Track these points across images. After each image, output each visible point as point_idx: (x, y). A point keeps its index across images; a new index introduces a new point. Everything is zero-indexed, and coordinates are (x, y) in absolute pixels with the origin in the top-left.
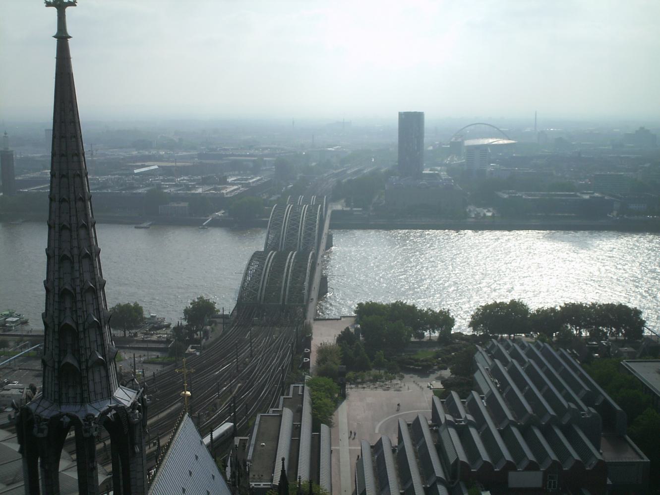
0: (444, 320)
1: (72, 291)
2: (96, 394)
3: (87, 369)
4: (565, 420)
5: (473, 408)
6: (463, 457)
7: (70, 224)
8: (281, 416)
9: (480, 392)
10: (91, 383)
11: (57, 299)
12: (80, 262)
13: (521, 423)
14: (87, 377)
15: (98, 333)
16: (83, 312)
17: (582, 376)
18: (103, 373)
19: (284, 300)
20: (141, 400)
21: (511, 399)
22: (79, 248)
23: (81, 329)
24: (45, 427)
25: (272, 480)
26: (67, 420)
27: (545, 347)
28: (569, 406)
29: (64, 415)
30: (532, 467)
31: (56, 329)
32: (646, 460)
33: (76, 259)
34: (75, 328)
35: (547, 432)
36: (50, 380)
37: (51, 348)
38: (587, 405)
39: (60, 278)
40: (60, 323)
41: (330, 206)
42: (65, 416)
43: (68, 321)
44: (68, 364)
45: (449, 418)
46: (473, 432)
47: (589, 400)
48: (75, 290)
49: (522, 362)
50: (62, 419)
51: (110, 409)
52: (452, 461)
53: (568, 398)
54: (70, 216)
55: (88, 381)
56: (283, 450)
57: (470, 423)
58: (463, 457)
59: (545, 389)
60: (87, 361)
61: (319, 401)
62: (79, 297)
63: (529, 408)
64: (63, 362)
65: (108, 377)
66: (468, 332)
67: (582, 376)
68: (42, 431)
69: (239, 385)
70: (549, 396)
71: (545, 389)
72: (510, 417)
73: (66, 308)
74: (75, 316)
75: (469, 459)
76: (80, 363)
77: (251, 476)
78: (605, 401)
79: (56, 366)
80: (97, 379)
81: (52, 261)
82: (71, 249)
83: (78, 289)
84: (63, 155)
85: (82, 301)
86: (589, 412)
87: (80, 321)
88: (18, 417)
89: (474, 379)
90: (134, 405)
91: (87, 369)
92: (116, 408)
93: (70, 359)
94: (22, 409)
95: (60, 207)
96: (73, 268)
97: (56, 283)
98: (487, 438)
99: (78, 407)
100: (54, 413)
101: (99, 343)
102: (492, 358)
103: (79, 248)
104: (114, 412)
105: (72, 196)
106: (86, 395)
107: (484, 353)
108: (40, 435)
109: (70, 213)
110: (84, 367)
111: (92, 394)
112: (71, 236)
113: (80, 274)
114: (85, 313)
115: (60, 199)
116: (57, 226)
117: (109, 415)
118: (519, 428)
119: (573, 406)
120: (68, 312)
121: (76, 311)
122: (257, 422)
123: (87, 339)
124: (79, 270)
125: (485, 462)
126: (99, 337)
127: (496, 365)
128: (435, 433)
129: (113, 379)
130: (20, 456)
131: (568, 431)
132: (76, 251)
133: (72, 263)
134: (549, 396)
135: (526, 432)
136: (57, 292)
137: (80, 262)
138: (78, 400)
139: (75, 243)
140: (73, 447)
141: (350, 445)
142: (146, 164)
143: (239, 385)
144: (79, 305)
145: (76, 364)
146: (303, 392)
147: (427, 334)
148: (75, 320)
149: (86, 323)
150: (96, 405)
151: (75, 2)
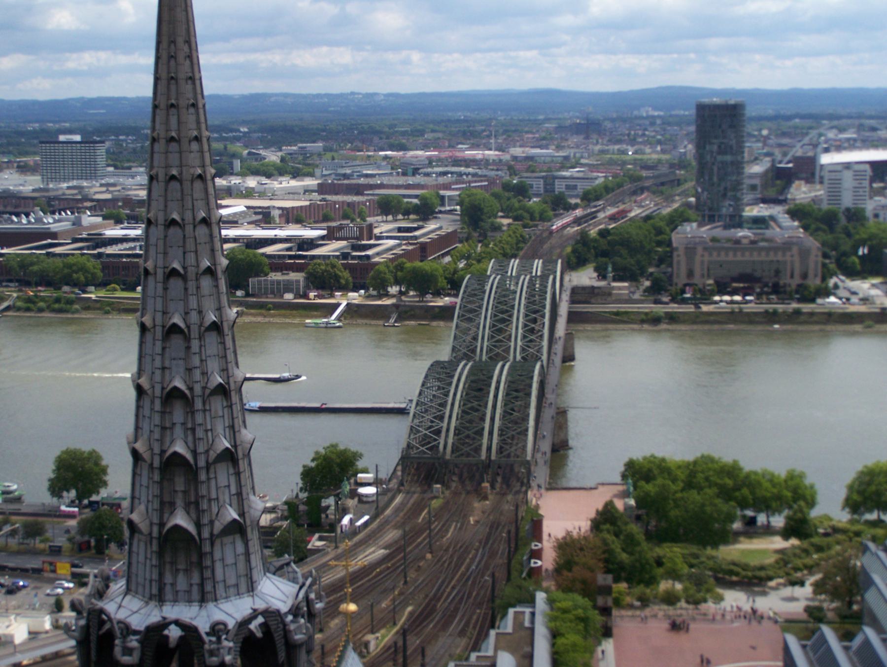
1: (187, 392)
2: (226, 587)
3: (212, 539)
7: (184, 268)
10: (218, 567)
11: (158, 406)
14: (212, 553)
15: (231, 471)
16: (206, 431)
18: (240, 548)
22: (200, 312)
23: (202, 463)
26: (174, 633)
29: (170, 623)
31: (157, 463)
33: (194, 334)
36: (141, 558)
37: (144, 498)
39: (163, 368)
40: (163, 452)
43: (179, 448)
44: (177, 527)
48: (191, 389)
50: (166, 632)
54: (184, 253)
55: (213, 562)
60: (212, 522)
62: (198, 404)
65: (247, 554)
68: (128, 651)
73: (174, 424)
74: (190, 438)
76: (198, 525)
79: (155, 533)
80: (230, 560)
82: (186, 313)
83: (198, 389)
84: (172, 139)
85: (205, 411)
87: (201, 449)
90: (295, 611)
91: (212, 539)
93: (181, 519)
95: (166, 237)
96: (188, 348)
97: (158, 377)
99: (195, 608)
101: (233, 490)
103: (200, 312)
104: (260, 620)
106: (208, 588)
108: (126, 659)
109: (184, 247)
110: (206, 534)
112: (186, 289)
113: (202, 361)
114: (210, 434)
115: (166, 221)
116: (160, 272)
117: (253, 626)
120: (178, 431)
121: (193, 430)
123: (213, 482)
124: (200, 353)
126: (233, 480)
133: (187, 339)
136: (158, 392)
139: (193, 303)
144: (199, 418)
148: (191, 445)
149: (211, 452)
150: (227, 606)
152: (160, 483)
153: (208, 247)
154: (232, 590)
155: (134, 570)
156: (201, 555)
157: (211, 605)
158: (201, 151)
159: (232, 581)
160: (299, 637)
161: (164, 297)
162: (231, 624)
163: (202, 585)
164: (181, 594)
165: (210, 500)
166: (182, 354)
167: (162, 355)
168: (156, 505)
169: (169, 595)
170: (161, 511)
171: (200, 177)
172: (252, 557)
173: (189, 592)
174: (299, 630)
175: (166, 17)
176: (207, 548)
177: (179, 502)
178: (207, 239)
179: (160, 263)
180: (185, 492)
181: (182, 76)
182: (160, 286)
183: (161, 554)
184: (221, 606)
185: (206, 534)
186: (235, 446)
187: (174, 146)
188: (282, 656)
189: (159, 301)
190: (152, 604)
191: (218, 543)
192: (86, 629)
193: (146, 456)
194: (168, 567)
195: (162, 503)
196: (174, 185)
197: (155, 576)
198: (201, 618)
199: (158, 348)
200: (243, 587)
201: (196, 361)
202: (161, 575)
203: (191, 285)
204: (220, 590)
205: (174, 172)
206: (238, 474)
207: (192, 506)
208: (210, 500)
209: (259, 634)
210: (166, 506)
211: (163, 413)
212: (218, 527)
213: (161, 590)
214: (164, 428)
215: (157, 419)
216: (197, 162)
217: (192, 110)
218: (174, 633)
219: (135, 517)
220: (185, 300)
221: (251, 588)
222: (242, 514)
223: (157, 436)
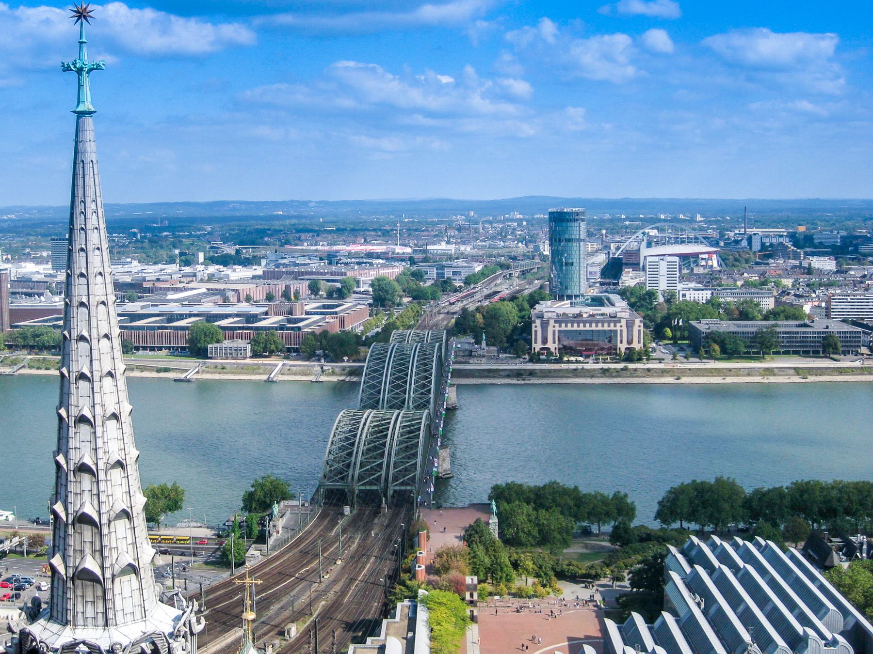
0: (620, 508)
3: (114, 577)
9: (675, 613)
10: (118, 599)
15: (128, 526)
16: (108, 496)
17: (822, 588)
19: (386, 480)
22: (103, 406)
23: (104, 521)
27: (767, 545)
28: (804, 631)
29: (80, 643)
33: (99, 421)
34: (97, 520)
42: (81, 645)
50: (77, 648)
53: (804, 620)
59: (769, 607)
61: (439, 627)
62: (102, 476)
66: (655, 525)
67: (822, 588)
69: (323, 603)
71: (769, 607)
74: (96, 502)
76: (103, 568)
80: (127, 594)
83: (101, 465)
85: (107, 481)
88: (16, 644)
101: (130, 541)
102: (691, 562)
103: (103, 406)
106: (110, 615)
107: (680, 557)
111: (120, 615)
112: (93, 388)
113: (104, 443)
114: (110, 497)
119: (811, 632)
123: (113, 535)
126: (129, 532)
127: (697, 574)
138: (100, 620)
139: (98, 399)
142: (190, 286)
143: (323, 603)
144: (102, 486)
145: (97, 571)
147: (595, 529)
149: (112, 512)
150: (123, 629)
153: (109, 356)
155: (55, 601)
159: (129, 609)
163: (105, 614)
164: (89, 620)
165: (111, 549)
169: (80, 621)
171: (103, 303)
176: (109, 585)
177: (88, 550)
178: (109, 350)
184: (119, 629)
185: (108, 574)
191: (117, 580)
194: (79, 599)
200: (138, 615)
207: (97, 553)
208: (111, 549)
212: (117, 569)
216: (102, 292)
217: (97, 252)
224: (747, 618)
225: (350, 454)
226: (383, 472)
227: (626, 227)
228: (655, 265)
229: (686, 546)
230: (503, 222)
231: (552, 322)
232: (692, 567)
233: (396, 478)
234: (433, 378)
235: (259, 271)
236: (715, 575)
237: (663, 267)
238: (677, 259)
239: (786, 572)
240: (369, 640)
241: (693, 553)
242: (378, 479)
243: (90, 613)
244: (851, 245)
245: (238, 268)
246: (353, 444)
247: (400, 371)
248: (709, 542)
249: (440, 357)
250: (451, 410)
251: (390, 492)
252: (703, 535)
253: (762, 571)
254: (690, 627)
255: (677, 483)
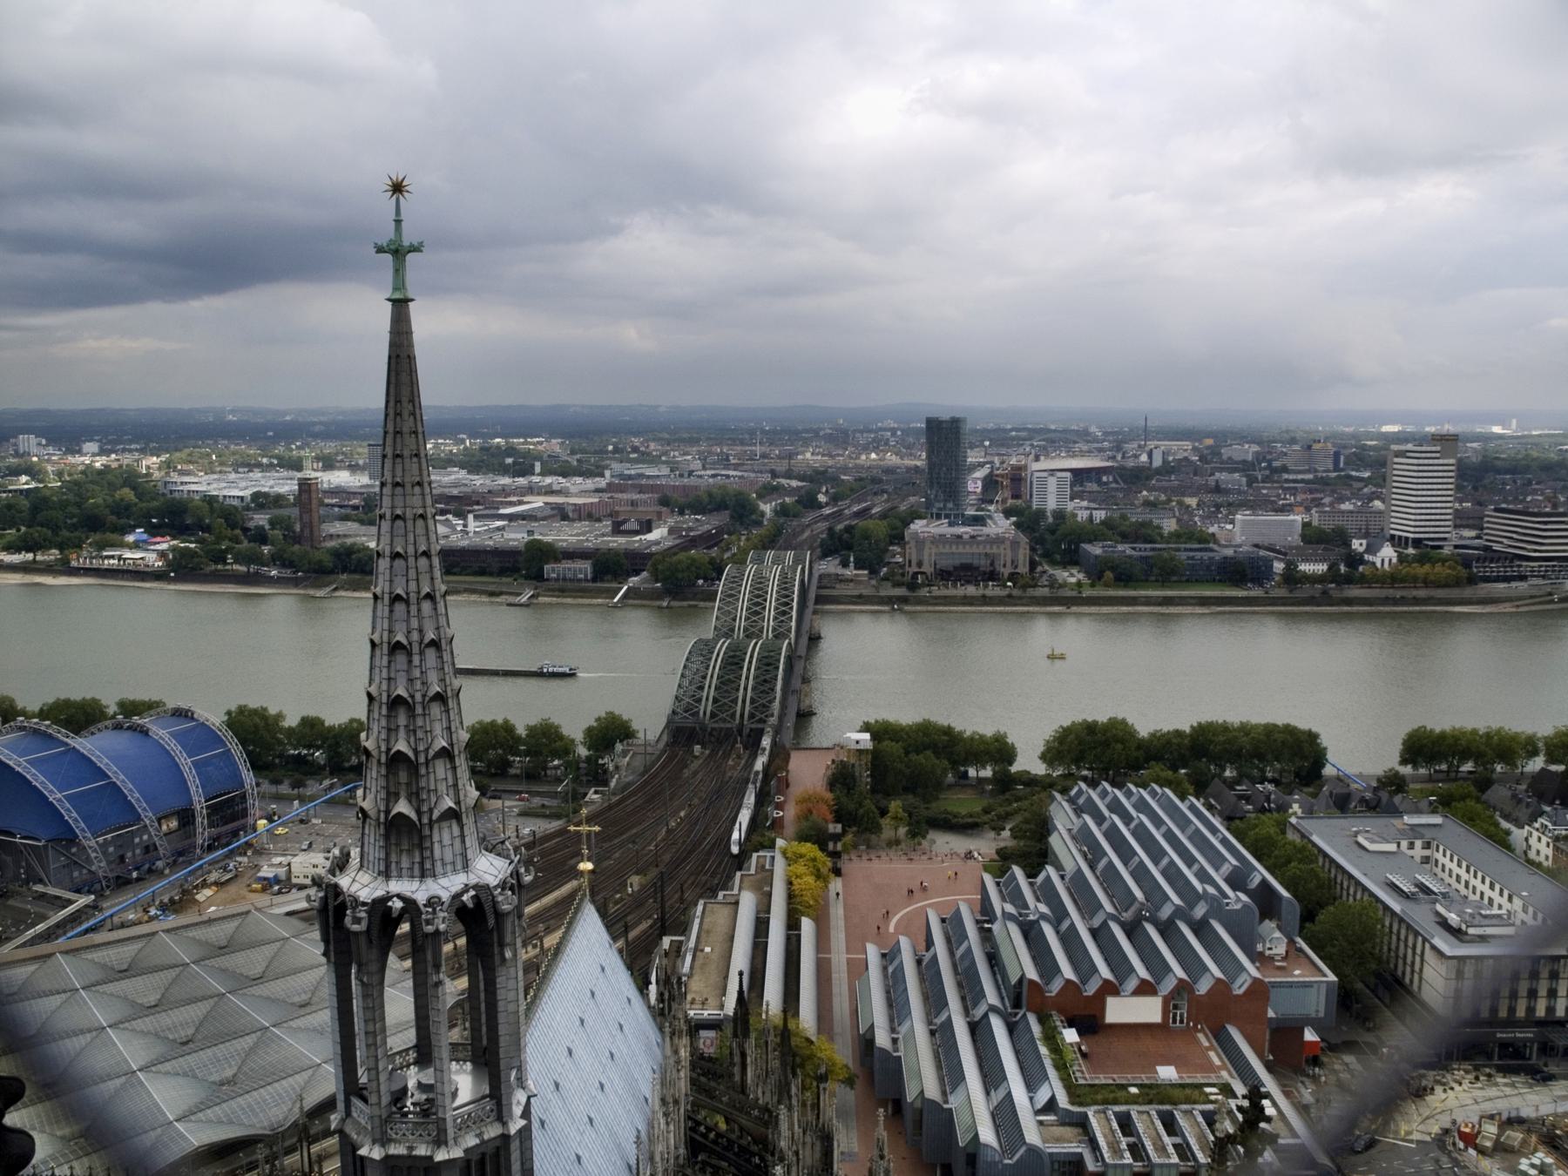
0: (1000, 752)
2: (444, 864)
4: (1200, 911)
5: (1047, 893)
6: (1032, 974)
8: (737, 903)
10: (436, 846)
11: (384, 712)
12: (421, 653)
13: (1127, 916)
17: (1224, 841)
18: (456, 830)
19: (742, 715)
20: (516, 874)
21: (1110, 879)
23: (422, 759)
24: (363, 915)
25: (722, 1007)
26: (397, 904)
27: (1164, 794)
30: (1145, 989)
31: (383, 759)
32: (1332, 977)
33: (416, 649)
35: (1167, 930)
38: (1235, 888)
40: (389, 750)
41: (816, 566)
45: (1010, 908)
46: (1048, 930)
47: (1237, 880)
48: (412, 697)
49: (1127, 819)
51: (466, 889)
52: (1014, 980)
53: (1203, 876)
56: (740, 959)
57: (1043, 917)
58: (1032, 974)
59: (1165, 861)
60: (431, 811)
62: (419, 710)
63: (1139, 894)
64: (394, 812)
65: (463, 837)
66: (1039, 769)
67: (1224, 841)
68: (357, 921)
70: (1172, 874)
72: (1109, 908)
75: (1041, 976)
76: (419, 813)
77: (689, 998)
78: (1264, 882)
79: (382, 819)
81: (378, 652)
83: (418, 697)
84: (398, 484)
86: (1239, 899)
87: (421, 748)
89: (1047, 844)
90: (503, 885)
92: (475, 887)
93: (403, 807)
94: (328, 885)
96: (410, 662)
97: (384, 687)
98: (1070, 940)
99: (416, 884)
100: (379, 893)
102: (1078, 811)
104: (472, 893)
105: (411, 550)
106: (428, 865)
107: (1065, 804)
108: (356, 928)
110: (425, 821)
111: (439, 864)
116: (386, 597)
117: (465, 898)
118: (1123, 925)
119: (1211, 890)
121: (415, 731)
122: (699, 913)
125: (1068, 981)
127: (1085, 823)
128: (986, 935)
129: (471, 841)
130: (324, 960)
131: (1201, 928)
132: (415, 636)
133: (410, 654)
134: (1172, 874)
135: (1132, 930)
136: (384, 699)
137: (421, 653)
138: (417, 872)
139: (415, 623)
140: (406, 947)
141: (848, 952)
142: (525, 499)
144: (420, 722)
145: (413, 816)
146: (772, 864)
147: (972, 772)
150: (443, 881)
151: (421, 244)
152: (387, 776)
154: (449, 867)
156: (422, 838)
157: (429, 881)
158: (423, 494)
159: (449, 857)
160: (506, 907)
161: (390, 618)
162: (445, 896)
163: (422, 863)
166: (405, 667)
167: (389, 667)
168: (383, 795)
169: (394, 873)
170: (388, 801)
171: (421, 516)
172: (467, 839)
173: (411, 869)
174: (507, 901)
175: (393, 380)
176: (426, 832)
177: (403, 794)
179: (387, 590)
180: (408, 784)
181: (405, 430)
182: (387, 609)
183: (387, 837)
185: (425, 821)
186: (452, 745)
187: (399, 490)
188: (491, 922)
189: (386, 622)
190: (380, 879)
192: (325, 900)
193: (375, 753)
195: (388, 793)
196: (399, 523)
197: (382, 855)
198: (419, 891)
199: (385, 661)
200: (459, 866)
201: (417, 673)
202: (387, 854)
203: (413, 609)
204: (439, 869)
205: (399, 512)
206: (454, 768)
209: (471, 905)
210: (391, 797)
211: (388, 717)
212: (436, 814)
213: (388, 867)
214: (389, 730)
215: (384, 723)
218: (397, 904)
219: (366, 805)
220: (408, 621)
221: (466, 866)
222: (458, 803)
223: (383, 736)
224: (1140, 874)
225: (701, 688)
226: (739, 708)
227: (1013, 439)
228: (1043, 481)
229: (1073, 793)
230: (876, 431)
231: (928, 545)
232: (1079, 816)
233: (752, 716)
234: (795, 604)
235: (602, 483)
236: (1106, 825)
237: (1052, 483)
238: (1068, 474)
239: (1183, 823)
240: (721, 894)
241: (1081, 801)
242: (733, 715)
243: (405, 864)
244: (1264, 459)
245: (579, 480)
246: (704, 677)
247: (758, 596)
248: (1099, 789)
249: (802, 581)
250: (815, 639)
251: (746, 731)
252: (1093, 784)
253: (1158, 822)
254: (1078, 886)
255: (1066, 723)
